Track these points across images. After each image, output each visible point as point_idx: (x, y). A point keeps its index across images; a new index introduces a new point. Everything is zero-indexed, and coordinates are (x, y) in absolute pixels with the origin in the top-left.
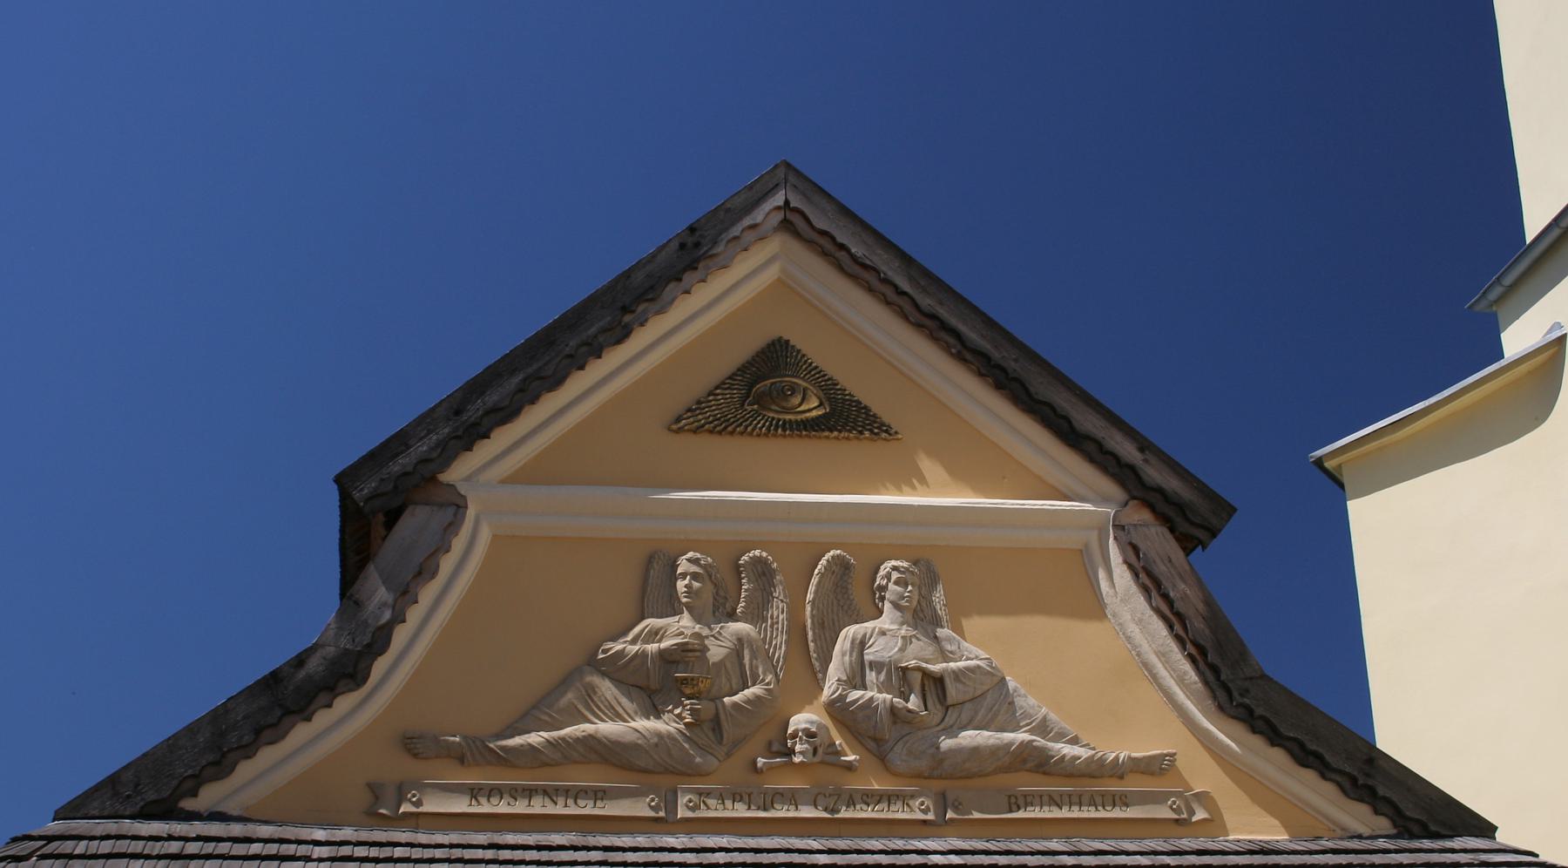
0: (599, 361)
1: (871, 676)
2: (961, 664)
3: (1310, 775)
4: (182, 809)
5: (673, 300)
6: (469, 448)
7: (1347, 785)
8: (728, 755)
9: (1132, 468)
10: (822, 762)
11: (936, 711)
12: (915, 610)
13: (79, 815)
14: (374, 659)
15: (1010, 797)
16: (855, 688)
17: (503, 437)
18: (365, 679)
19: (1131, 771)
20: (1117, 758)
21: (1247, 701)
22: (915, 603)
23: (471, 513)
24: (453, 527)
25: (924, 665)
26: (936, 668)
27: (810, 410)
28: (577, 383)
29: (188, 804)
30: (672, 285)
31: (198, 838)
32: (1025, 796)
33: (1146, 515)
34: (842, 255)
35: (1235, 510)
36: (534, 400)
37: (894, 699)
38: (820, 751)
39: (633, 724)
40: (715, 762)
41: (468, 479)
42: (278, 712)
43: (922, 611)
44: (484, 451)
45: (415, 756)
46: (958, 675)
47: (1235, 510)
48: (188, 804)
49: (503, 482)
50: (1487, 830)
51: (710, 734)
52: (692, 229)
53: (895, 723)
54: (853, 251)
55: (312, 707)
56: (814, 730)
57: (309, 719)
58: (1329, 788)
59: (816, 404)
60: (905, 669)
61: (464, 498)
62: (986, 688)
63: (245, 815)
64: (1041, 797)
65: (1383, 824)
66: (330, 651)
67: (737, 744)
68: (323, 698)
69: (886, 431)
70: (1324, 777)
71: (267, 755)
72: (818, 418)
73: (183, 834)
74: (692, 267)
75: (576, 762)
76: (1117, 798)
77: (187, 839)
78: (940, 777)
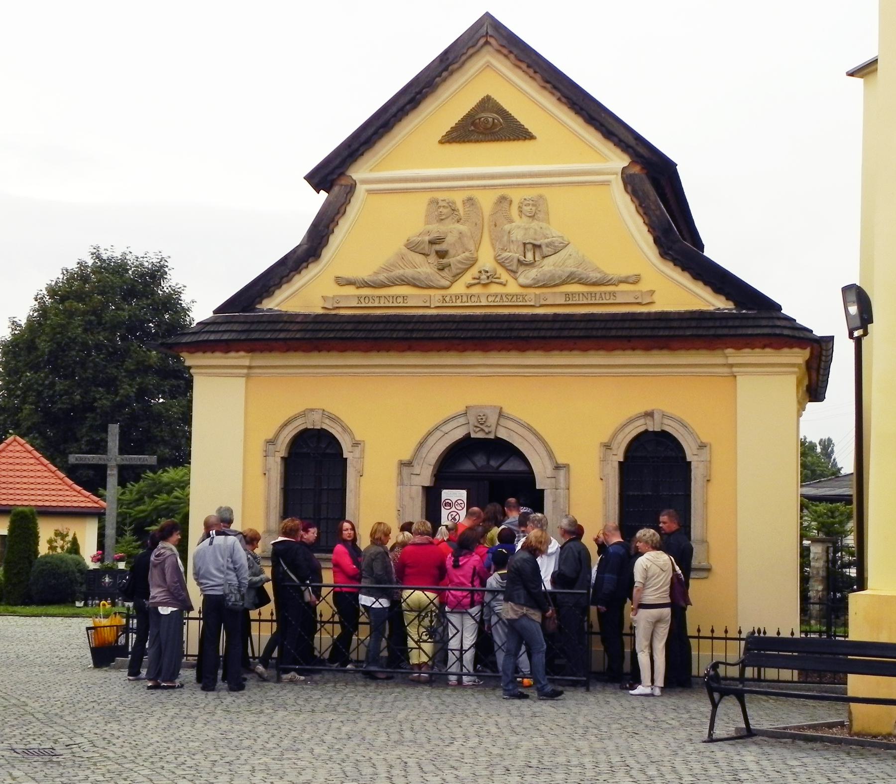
2: (549, 240)
39: (419, 270)
50: (779, 308)
55: (300, 268)
64: (579, 294)
68: (305, 264)
69: (529, 135)
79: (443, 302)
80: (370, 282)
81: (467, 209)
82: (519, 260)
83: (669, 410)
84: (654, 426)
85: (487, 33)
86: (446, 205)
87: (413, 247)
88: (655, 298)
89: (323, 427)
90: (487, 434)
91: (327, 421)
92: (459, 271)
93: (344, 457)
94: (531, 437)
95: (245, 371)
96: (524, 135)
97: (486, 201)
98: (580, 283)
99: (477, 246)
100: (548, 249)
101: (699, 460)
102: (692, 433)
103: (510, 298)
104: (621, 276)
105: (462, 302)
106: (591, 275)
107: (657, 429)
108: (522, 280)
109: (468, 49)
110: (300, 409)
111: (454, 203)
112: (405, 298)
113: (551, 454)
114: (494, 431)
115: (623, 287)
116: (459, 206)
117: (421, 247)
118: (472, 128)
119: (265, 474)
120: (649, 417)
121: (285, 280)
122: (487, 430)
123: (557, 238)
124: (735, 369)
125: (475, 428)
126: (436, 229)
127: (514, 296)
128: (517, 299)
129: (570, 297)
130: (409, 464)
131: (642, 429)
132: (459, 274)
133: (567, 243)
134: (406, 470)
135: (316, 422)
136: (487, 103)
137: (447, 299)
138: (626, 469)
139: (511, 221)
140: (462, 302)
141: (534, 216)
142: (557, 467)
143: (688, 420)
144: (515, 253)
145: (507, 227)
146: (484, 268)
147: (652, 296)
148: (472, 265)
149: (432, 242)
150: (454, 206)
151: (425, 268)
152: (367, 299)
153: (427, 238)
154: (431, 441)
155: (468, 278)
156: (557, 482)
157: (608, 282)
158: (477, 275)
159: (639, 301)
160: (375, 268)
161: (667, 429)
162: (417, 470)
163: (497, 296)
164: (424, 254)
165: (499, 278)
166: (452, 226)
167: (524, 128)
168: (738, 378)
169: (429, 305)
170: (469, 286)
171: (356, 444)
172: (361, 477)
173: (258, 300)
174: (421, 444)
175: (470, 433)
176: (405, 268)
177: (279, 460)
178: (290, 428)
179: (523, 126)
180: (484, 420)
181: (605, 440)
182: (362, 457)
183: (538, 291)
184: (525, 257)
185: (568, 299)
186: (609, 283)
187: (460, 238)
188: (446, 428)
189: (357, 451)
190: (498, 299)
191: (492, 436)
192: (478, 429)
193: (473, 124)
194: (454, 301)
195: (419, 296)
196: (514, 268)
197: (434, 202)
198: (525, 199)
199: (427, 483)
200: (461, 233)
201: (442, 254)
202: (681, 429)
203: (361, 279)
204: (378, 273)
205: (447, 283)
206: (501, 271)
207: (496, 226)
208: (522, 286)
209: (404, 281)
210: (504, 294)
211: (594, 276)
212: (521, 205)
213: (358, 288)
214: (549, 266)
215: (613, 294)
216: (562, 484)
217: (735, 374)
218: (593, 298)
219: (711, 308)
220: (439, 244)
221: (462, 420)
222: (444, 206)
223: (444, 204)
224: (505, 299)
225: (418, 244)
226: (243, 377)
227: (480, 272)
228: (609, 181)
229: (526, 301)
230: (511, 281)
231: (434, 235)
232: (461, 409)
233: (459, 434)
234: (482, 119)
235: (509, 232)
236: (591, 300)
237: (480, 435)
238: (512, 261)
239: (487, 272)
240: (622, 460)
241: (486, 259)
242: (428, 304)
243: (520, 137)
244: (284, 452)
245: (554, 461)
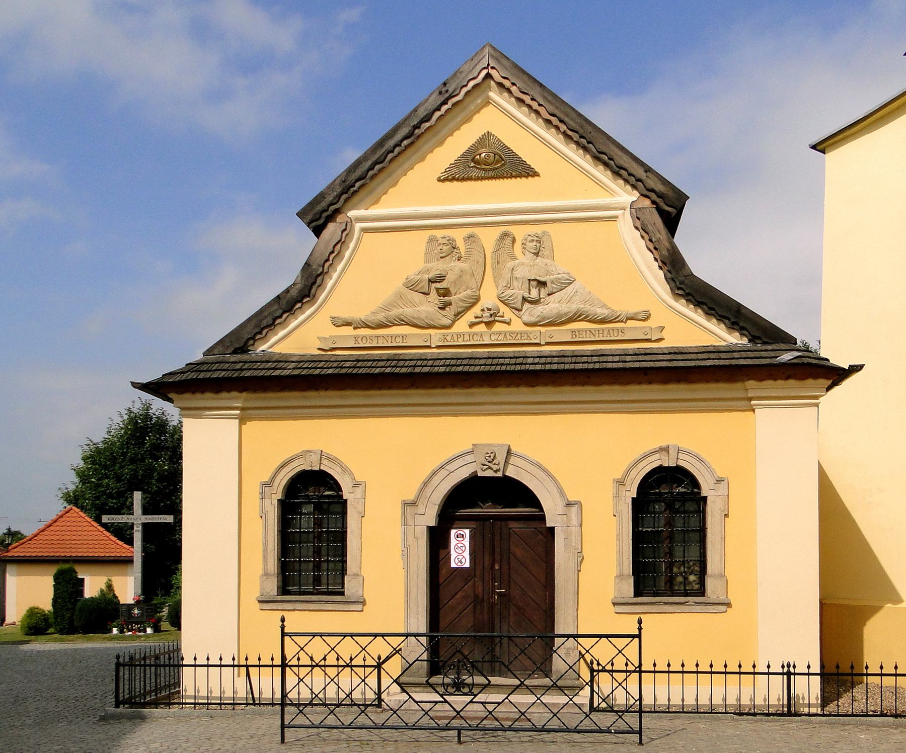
1: (515, 283)
15: (572, 332)
25: (538, 278)
32: (579, 331)
33: (647, 203)
35: (689, 198)
42: (281, 311)
47: (689, 198)
52: (445, 84)
66: (299, 286)
68: (299, 305)
75: (397, 325)
76: (620, 331)
80: (369, 322)
81: (468, 247)
82: (523, 297)
83: (683, 446)
84: (668, 461)
85: (488, 65)
86: (447, 242)
87: (412, 286)
88: (664, 334)
89: (322, 468)
90: (496, 472)
92: (460, 310)
94: (542, 475)
95: (238, 412)
96: (527, 171)
97: (489, 238)
98: (586, 321)
99: (479, 284)
100: (553, 285)
101: (716, 494)
102: (708, 467)
103: (514, 336)
104: (630, 312)
106: (597, 312)
107: (673, 464)
108: (526, 318)
109: (468, 82)
110: (297, 451)
111: (454, 241)
112: (404, 338)
113: (562, 493)
114: (502, 469)
115: (631, 323)
116: (460, 244)
117: (420, 286)
118: (472, 165)
119: (261, 517)
123: (563, 275)
124: (753, 402)
125: (482, 466)
126: (437, 267)
127: (518, 333)
128: (521, 336)
129: (577, 334)
130: (414, 504)
131: (655, 465)
132: (464, 311)
133: (573, 279)
134: (409, 510)
136: (486, 139)
137: (449, 338)
138: (640, 506)
139: (514, 258)
141: (538, 253)
142: (569, 504)
143: (704, 456)
144: (518, 292)
145: (510, 264)
146: (488, 306)
147: (661, 332)
148: (473, 304)
149: (431, 281)
150: (454, 244)
151: (427, 307)
152: (364, 338)
153: (426, 277)
154: (436, 479)
155: (469, 317)
156: (569, 519)
157: (616, 318)
158: (479, 314)
159: (648, 337)
160: (374, 308)
161: (682, 463)
162: (421, 509)
164: (424, 293)
165: (503, 317)
166: (453, 264)
167: (527, 164)
168: (756, 410)
169: (429, 345)
170: (472, 325)
171: (356, 485)
172: (363, 518)
174: (425, 484)
175: (476, 471)
176: (405, 308)
178: (286, 469)
179: (525, 162)
180: (492, 458)
181: (619, 476)
183: (543, 329)
184: (529, 293)
186: (616, 320)
187: (460, 276)
188: (451, 467)
189: (359, 490)
190: (501, 337)
191: (500, 474)
192: (486, 467)
193: (473, 160)
195: (419, 335)
196: (518, 306)
197: (432, 240)
198: (529, 235)
199: (433, 523)
200: (462, 271)
201: (445, 293)
203: (358, 319)
204: (377, 313)
205: (448, 322)
206: (503, 309)
207: (498, 263)
208: (526, 324)
209: (404, 321)
210: (508, 332)
211: (601, 312)
212: (525, 242)
213: (355, 328)
214: (553, 306)
215: (622, 331)
216: (575, 521)
217: (754, 407)
218: (601, 335)
219: (724, 344)
220: (442, 282)
221: (469, 458)
222: (443, 244)
223: (445, 241)
224: (509, 337)
225: (418, 282)
226: (236, 418)
227: (483, 310)
228: (617, 217)
229: (531, 339)
230: (514, 318)
231: (432, 275)
232: (469, 447)
233: (464, 473)
234: (484, 154)
235: (513, 269)
236: (599, 337)
237: (489, 473)
238: (515, 298)
239: (489, 310)
240: (635, 496)
241: (489, 298)
242: (428, 344)
243: (523, 173)
244: (281, 495)
245: (566, 499)
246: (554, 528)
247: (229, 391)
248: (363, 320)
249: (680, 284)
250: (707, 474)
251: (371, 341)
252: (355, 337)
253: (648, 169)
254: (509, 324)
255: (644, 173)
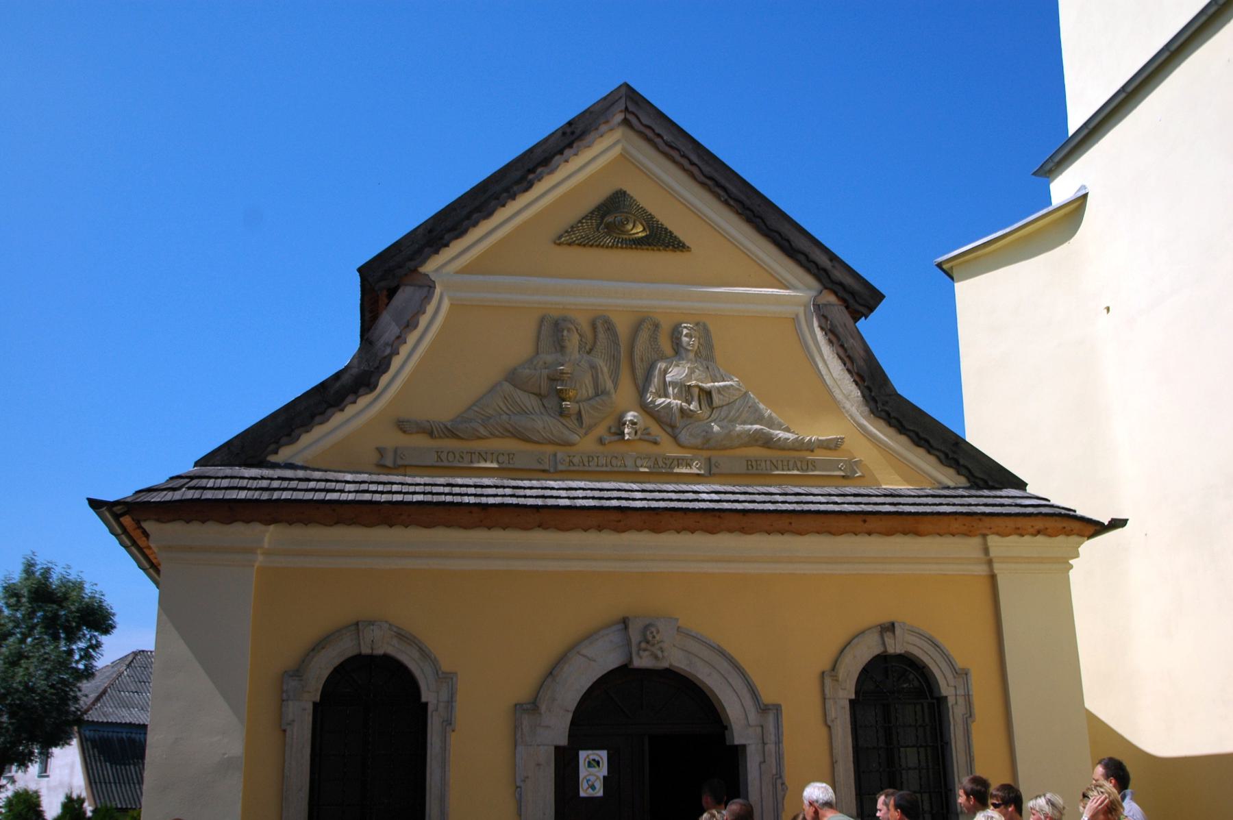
0: (514, 202)
1: (670, 390)
3: (921, 451)
4: (269, 461)
5: (558, 167)
6: (437, 252)
7: (942, 456)
8: (586, 434)
9: (825, 270)
10: (640, 439)
11: (706, 411)
12: (696, 352)
13: (209, 464)
14: (381, 376)
16: (660, 397)
17: (457, 246)
18: (375, 387)
19: (819, 447)
20: (811, 439)
21: (887, 409)
22: (696, 348)
23: (438, 291)
24: (428, 298)
25: (700, 384)
26: (708, 385)
27: (637, 233)
28: (501, 215)
29: (272, 458)
30: (558, 157)
31: (279, 478)
33: (832, 299)
34: (658, 140)
36: (475, 224)
37: (683, 404)
38: (639, 433)
40: (579, 438)
41: (437, 270)
43: (700, 352)
44: (446, 254)
45: (405, 432)
46: (719, 390)
48: (272, 458)
49: (457, 273)
50: (1021, 485)
51: (576, 422)
53: (682, 417)
54: (665, 138)
55: (345, 403)
56: (635, 421)
57: (342, 410)
58: (932, 459)
59: (641, 229)
60: (689, 386)
61: (434, 282)
62: (736, 398)
63: (305, 465)
64: (766, 461)
65: (962, 481)
67: (590, 428)
68: (351, 398)
70: (929, 452)
71: (318, 431)
72: (642, 238)
73: (270, 476)
74: (570, 145)
75: (497, 437)
77: (272, 479)
78: (708, 449)
79: (569, 465)
84: (895, 647)
91: (395, 642)
93: (424, 699)
103: (668, 462)
105: (598, 466)
107: (899, 650)
120: (888, 633)
121: (318, 419)
122: (659, 654)
131: (877, 650)
135: (382, 644)
140: (598, 466)
142: (764, 709)
163: (650, 458)
173: (272, 447)
177: (310, 707)
181: (826, 666)
182: (451, 701)
185: (750, 467)
192: (647, 653)
194: (586, 464)
199: (563, 741)
202: (931, 651)
209: (507, 430)
240: (853, 697)
246: (744, 746)
247: (247, 521)
248: (449, 427)
249: (883, 405)
250: (943, 665)
251: (461, 460)
252: (437, 452)
253: (833, 257)
254: (656, 443)
255: (828, 262)
